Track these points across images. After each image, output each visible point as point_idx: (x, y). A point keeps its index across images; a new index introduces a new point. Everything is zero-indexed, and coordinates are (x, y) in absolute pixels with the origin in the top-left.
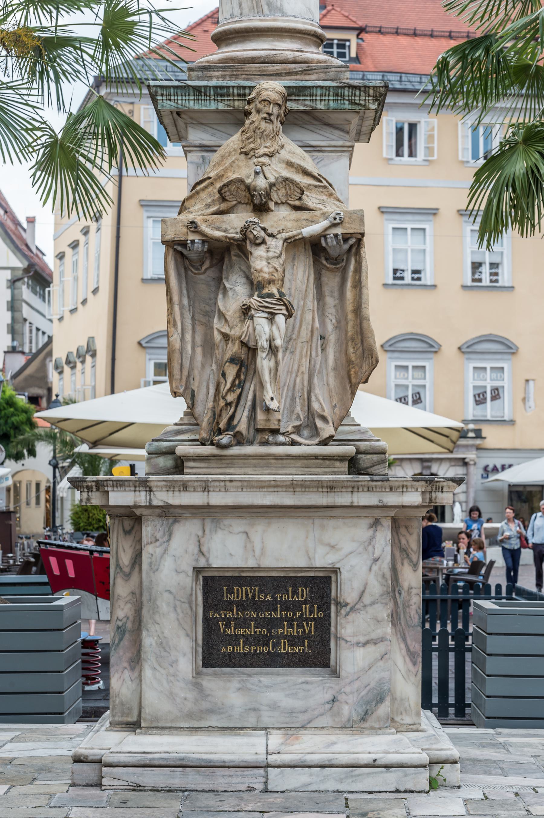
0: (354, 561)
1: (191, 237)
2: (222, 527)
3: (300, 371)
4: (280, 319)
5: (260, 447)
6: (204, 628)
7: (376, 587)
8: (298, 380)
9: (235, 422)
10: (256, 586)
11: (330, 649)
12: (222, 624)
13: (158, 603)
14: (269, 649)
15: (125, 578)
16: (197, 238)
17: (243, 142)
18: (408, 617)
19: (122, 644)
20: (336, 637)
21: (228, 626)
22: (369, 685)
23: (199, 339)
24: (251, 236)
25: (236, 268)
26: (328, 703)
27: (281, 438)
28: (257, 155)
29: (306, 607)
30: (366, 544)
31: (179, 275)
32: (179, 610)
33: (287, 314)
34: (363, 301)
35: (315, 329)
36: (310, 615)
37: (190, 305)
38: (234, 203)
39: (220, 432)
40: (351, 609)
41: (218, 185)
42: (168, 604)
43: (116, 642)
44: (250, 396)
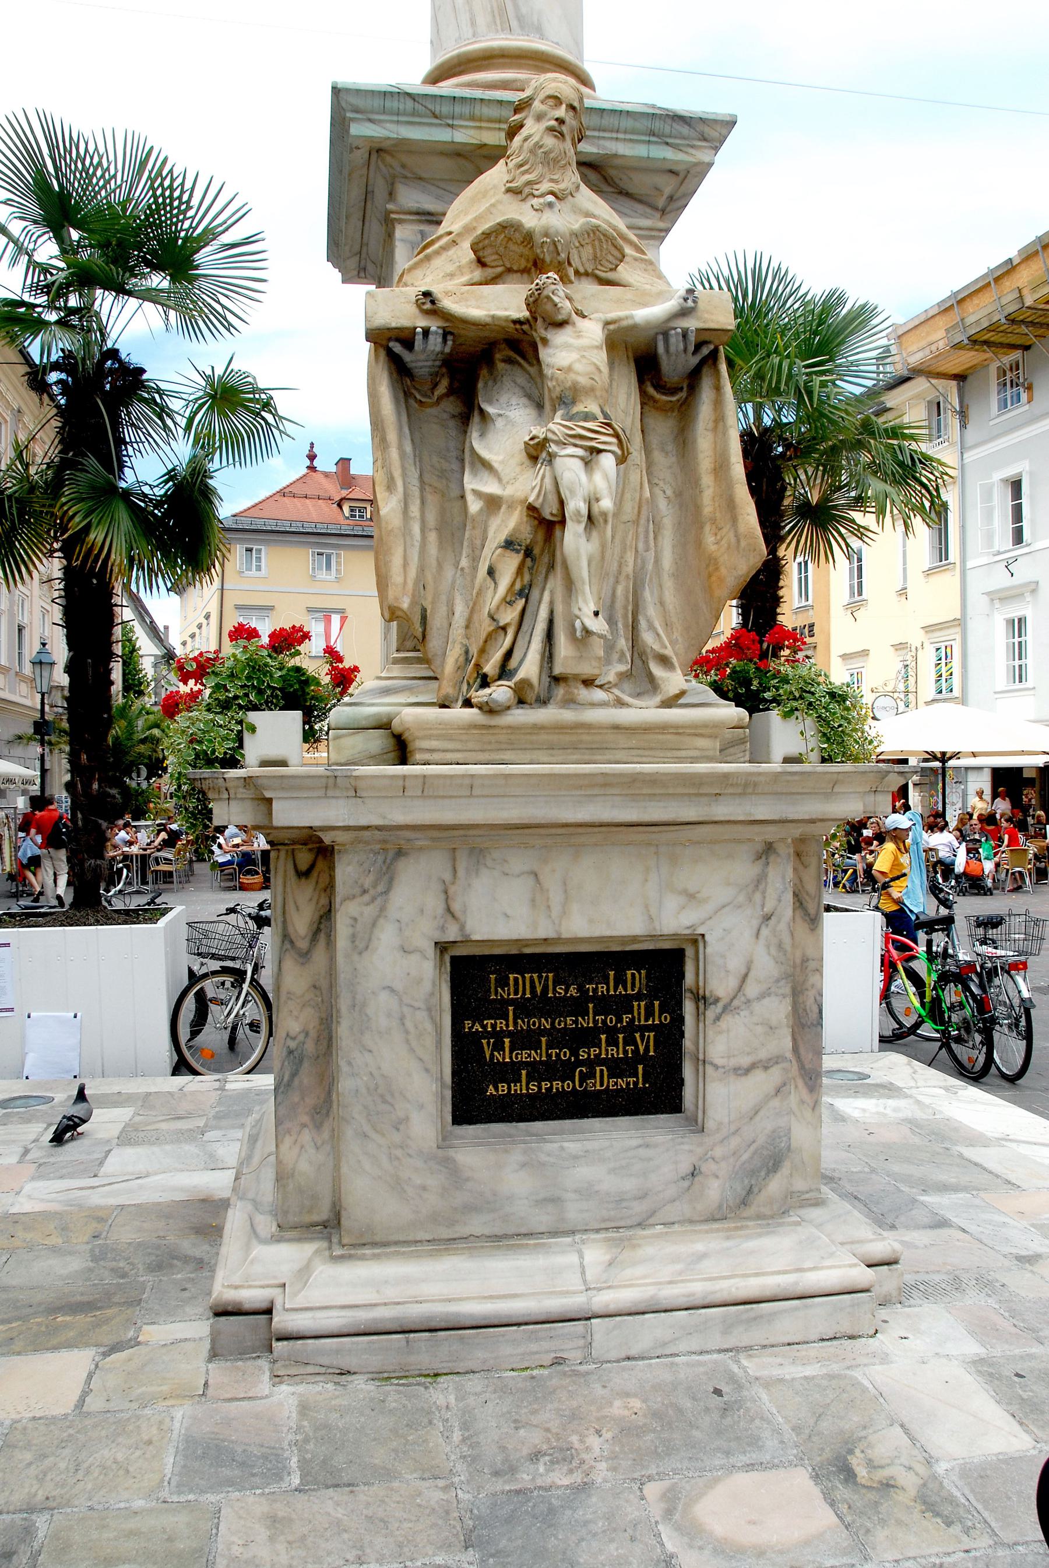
1: (421, 322)
2: (489, 863)
3: (624, 574)
4: (607, 461)
5: (561, 711)
7: (766, 966)
9: (513, 663)
11: (683, 1080)
12: (488, 1043)
13: (370, 1011)
14: (574, 1086)
15: (301, 960)
21: (499, 1046)
22: (754, 1142)
23: (432, 518)
26: (683, 1179)
27: (599, 695)
29: (639, 1005)
33: (619, 452)
35: (644, 501)
36: (646, 1020)
38: (500, 269)
39: (485, 683)
40: (725, 1008)
44: (543, 614)
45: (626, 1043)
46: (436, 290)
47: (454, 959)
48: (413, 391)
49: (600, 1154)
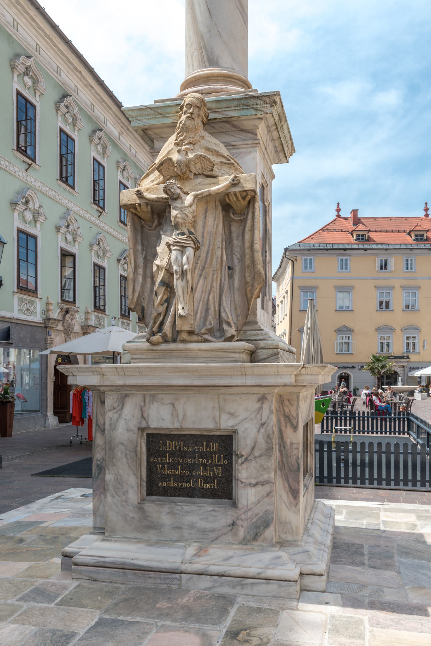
0: (247, 425)
4: (190, 252)
6: (147, 469)
8: (211, 297)
10: (182, 441)
11: (232, 486)
12: (159, 467)
13: (115, 452)
14: (190, 485)
18: (290, 464)
19: (99, 477)
20: (236, 479)
21: (163, 468)
22: (258, 514)
26: (229, 526)
30: (256, 412)
32: (129, 457)
33: (194, 247)
34: (255, 239)
36: (218, 462)
37: (143, 250)
40: (246, 459)
42: (122, 453)
43: (96, 475)
45: (210, 470)
47: (148, 435)
49: (200, 513)
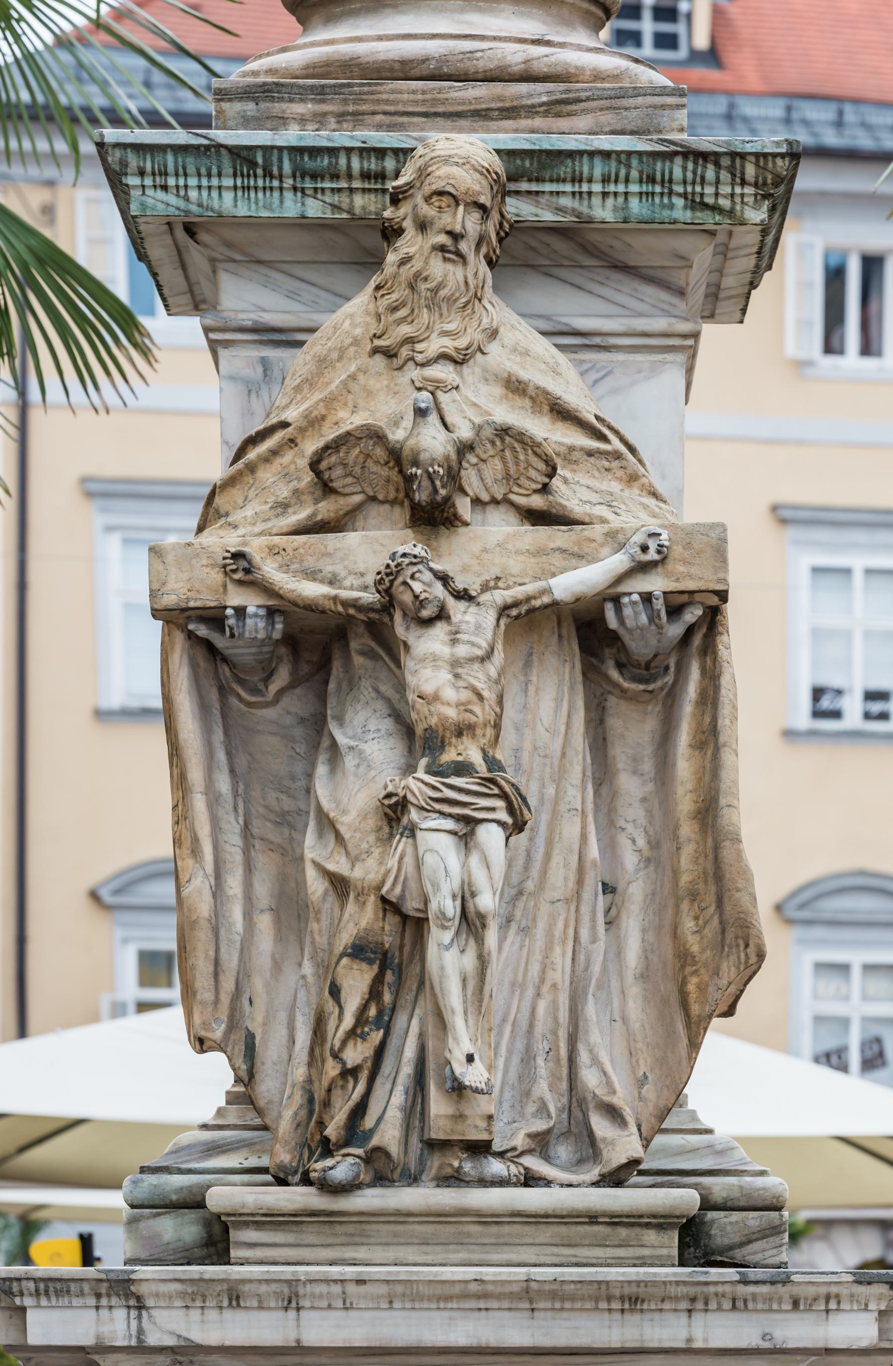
1: (235, 598)
4: (491, 836)
16: (252, 602)
17: (378, 317)
23: (263, 890)
24: (407, 598)
25: (366, 689)
28: (419, 358)
31: (203, 708)
37: (236, 794)
38: (357, 499)
41: (311, 446)
46: (255, 549)
48: (236, 687)
